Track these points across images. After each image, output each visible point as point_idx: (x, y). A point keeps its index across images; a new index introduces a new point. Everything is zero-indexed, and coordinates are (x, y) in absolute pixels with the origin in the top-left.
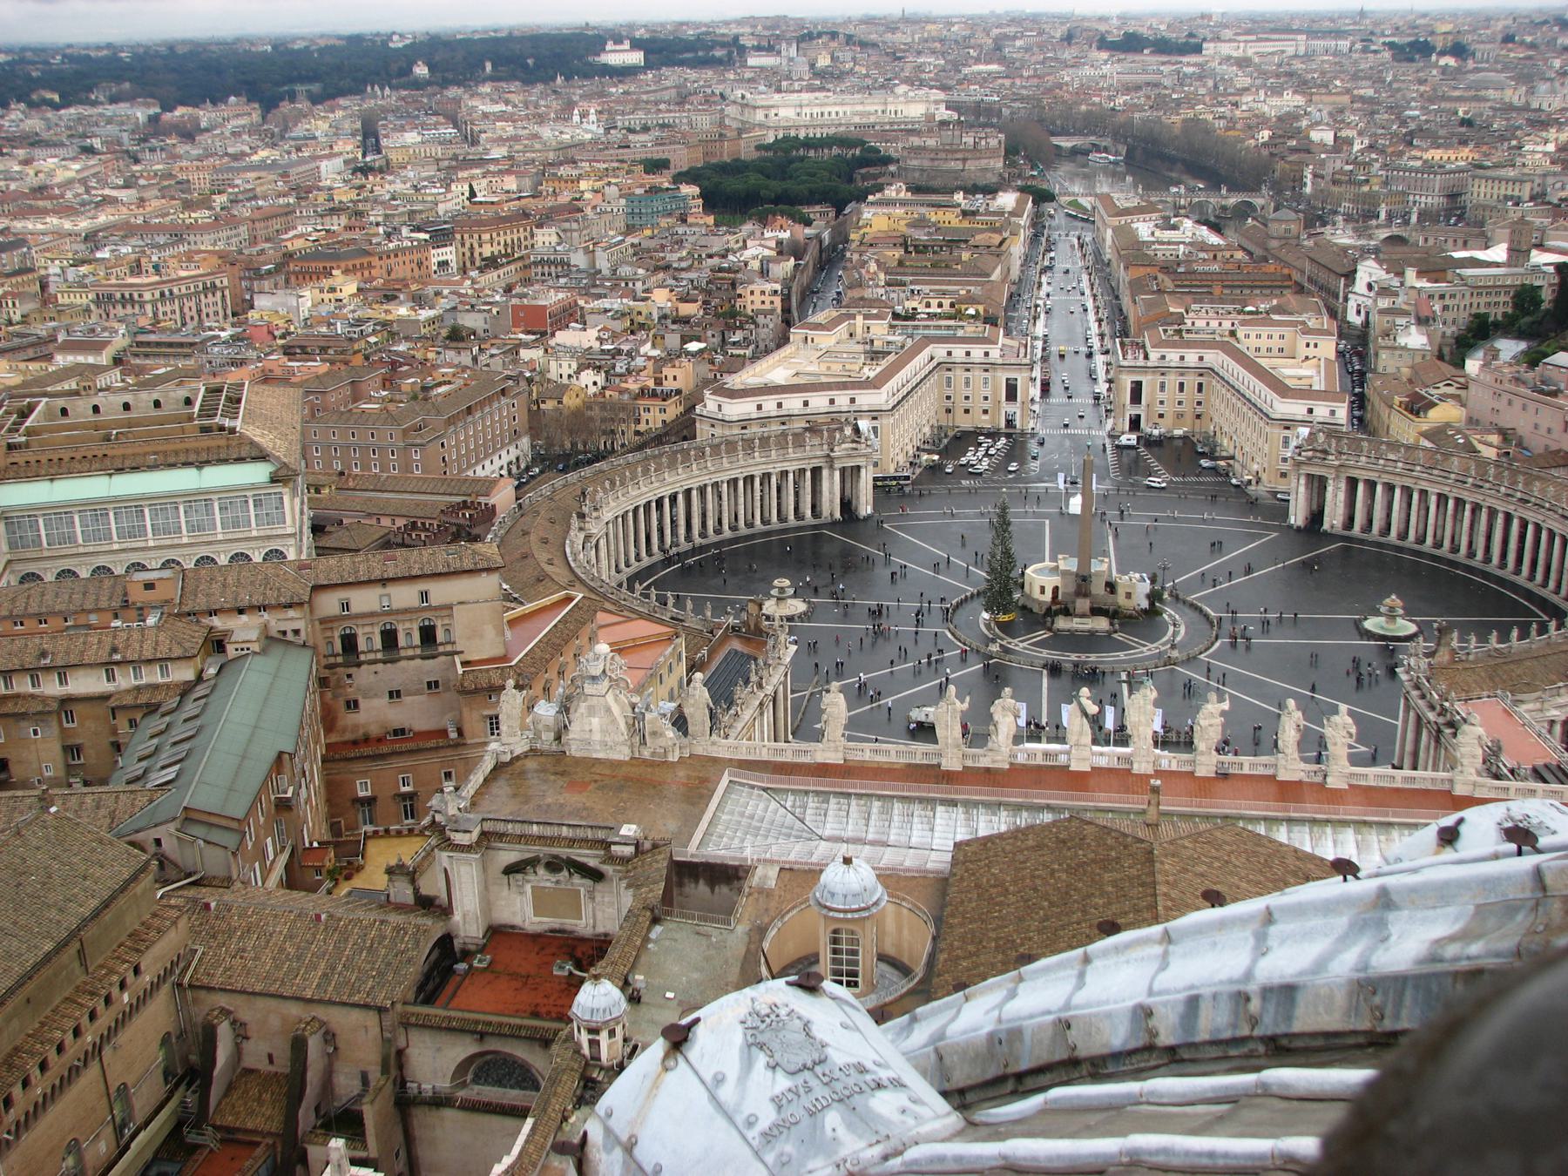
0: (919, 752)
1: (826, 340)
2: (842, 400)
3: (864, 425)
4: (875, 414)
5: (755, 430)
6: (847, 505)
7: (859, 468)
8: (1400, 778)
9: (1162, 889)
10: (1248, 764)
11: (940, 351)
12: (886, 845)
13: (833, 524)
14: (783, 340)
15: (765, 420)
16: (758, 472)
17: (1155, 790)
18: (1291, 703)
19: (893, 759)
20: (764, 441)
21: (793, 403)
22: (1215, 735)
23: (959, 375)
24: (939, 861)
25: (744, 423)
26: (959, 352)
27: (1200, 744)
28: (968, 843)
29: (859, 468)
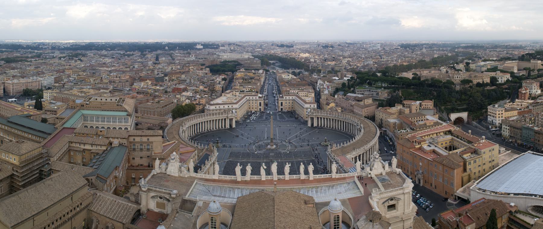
0: (233, 177)
1: (228, 95)
2: (230, 106)
3: (234, 111)
4: (236, 109)
5: (215, 112)
6: (231, 126)
7: (232, 119)
8: (323, 176)
9: (276, 207)
10: (295, 177)
11: (248, 97)
12: (225, 197)
13: (228, 129)
14: (221, 95)
15: (216, 110)
16: (214, 119)
17: (275, 185)
18: (302, 163)
19: (228, 178)
20: (216, 114)
21: (222, 107)
22: (288, 171)
23: (251, 102)
24: (234, 201)
25: (213, 110)
26: (251, 97)
27: (286, 173)
28: (240, 197)
29: (232, 119)
